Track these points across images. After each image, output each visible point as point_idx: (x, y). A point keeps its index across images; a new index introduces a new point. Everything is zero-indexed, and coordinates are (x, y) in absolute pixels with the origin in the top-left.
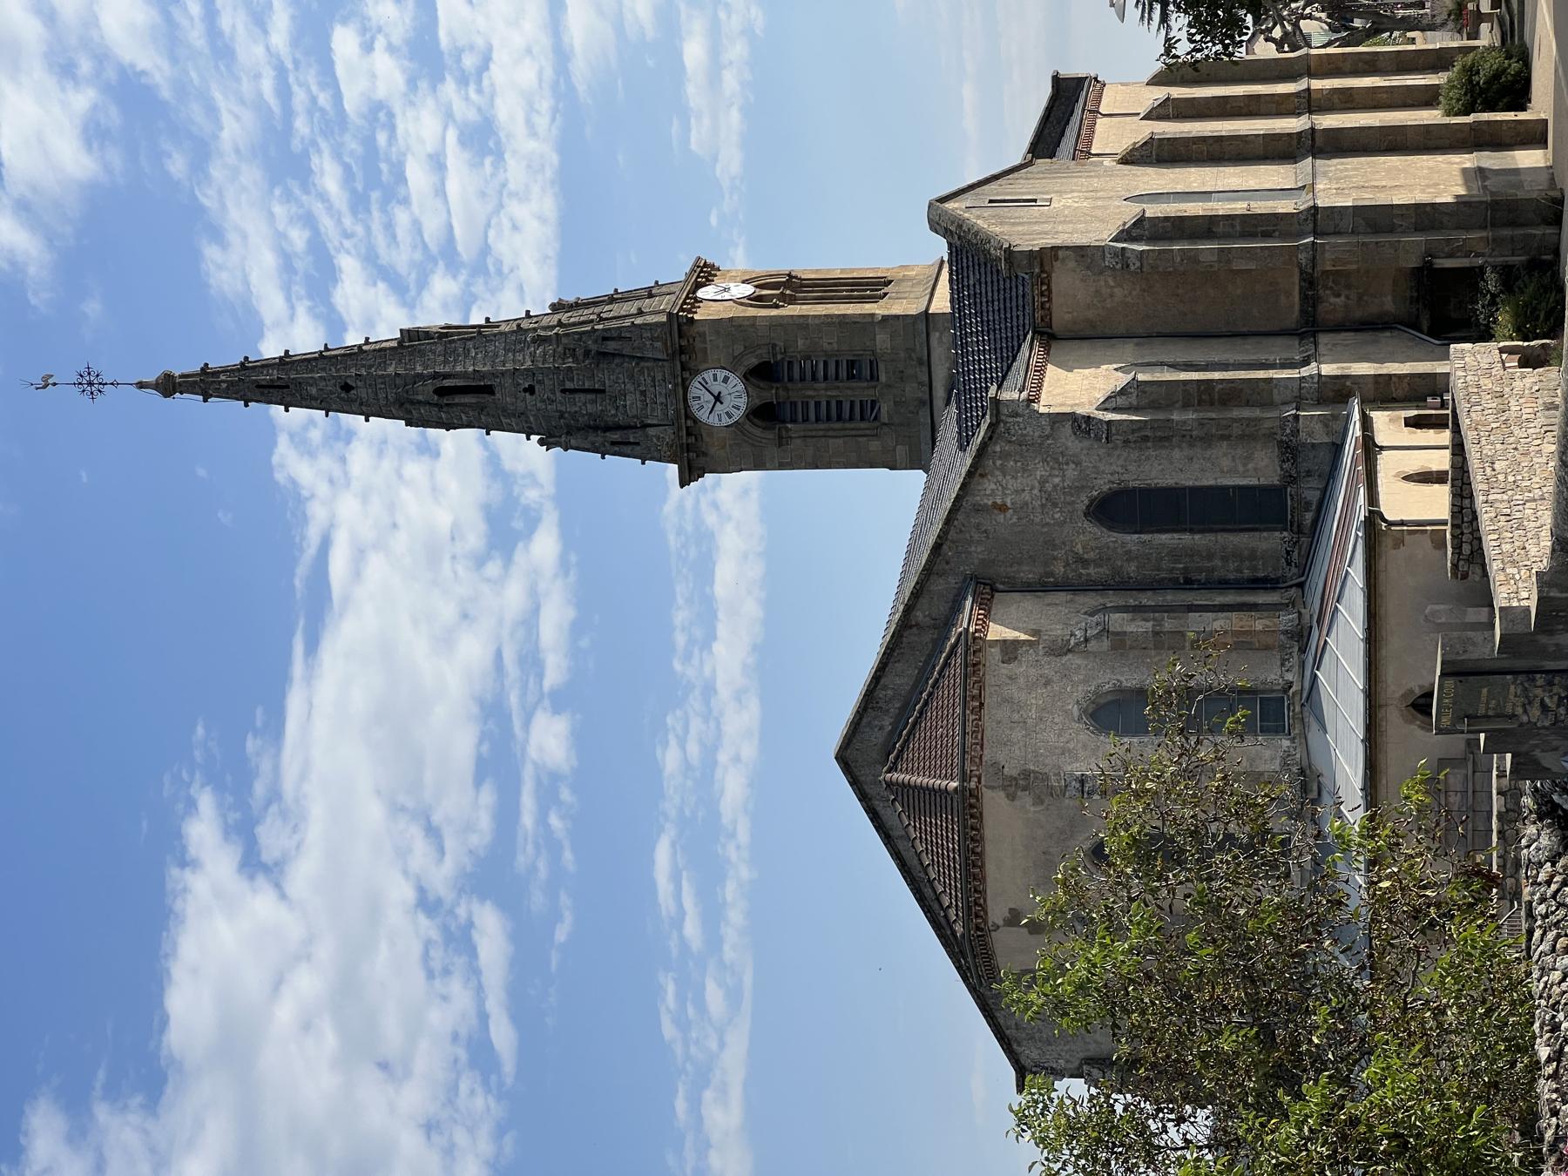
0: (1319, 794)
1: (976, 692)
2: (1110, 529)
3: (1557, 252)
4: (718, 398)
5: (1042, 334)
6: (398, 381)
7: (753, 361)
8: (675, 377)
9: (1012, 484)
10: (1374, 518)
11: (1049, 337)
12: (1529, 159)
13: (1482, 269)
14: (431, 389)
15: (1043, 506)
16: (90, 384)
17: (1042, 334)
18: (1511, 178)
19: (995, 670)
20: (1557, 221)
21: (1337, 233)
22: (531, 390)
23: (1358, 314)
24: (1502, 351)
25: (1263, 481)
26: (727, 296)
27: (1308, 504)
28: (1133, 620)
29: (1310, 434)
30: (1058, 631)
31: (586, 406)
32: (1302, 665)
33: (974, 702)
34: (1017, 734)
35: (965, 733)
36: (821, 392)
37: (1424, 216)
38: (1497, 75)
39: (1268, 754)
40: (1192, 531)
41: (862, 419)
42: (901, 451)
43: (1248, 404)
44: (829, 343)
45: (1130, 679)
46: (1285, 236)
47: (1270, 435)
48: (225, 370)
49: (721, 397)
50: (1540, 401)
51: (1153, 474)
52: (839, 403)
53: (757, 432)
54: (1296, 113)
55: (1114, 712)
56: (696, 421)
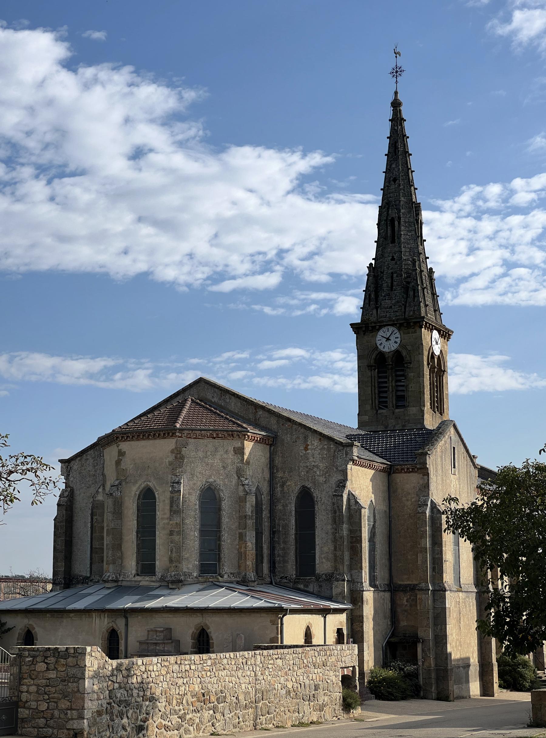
0: (171, 589)
1: (220, 435)
2: (297, 497)
3: (424, 698)
4: (388, 339)
5: (390, 469)
6: (398, 202)
7: (404, 354)
8: (397, 320)
9: (316, 452)
10: (284, 611)
11: (389, 472)
12: (475, 688)
13: (416, 664)
14: (394, 216)
15: (307, 467)
16: (397, 72)
18: (464, 680)
19: (230, 445)
20: (439, 699)
21: (434, 601)
22: (393, 259)
23: (399, 610)
24: (354, 667)
25: (317, 566)
26: (434, 343)
27: (307, 586)
28: (252, 506)
29: (336, 586)
30: (249, 472)
31: (386, 284)
32: (231, 582)
33: (215, 434)
34: (201, 454)
35: (201, 430)
36: (391, 384)
37: (441, 639)
38: (522, 676)
40: (296, 534)
41: (379, 402)
42: (366, 418)
43: (351, 559)
44: (412, 387)
45: (226, 505)
46: (433, 577)
47: (336, 569)
48: (403, 128)
49: (388, 341)
50: (320, 683)
52: (386, 392)
53: (374, 356)
55: (210, 498)
56: (378, 330)
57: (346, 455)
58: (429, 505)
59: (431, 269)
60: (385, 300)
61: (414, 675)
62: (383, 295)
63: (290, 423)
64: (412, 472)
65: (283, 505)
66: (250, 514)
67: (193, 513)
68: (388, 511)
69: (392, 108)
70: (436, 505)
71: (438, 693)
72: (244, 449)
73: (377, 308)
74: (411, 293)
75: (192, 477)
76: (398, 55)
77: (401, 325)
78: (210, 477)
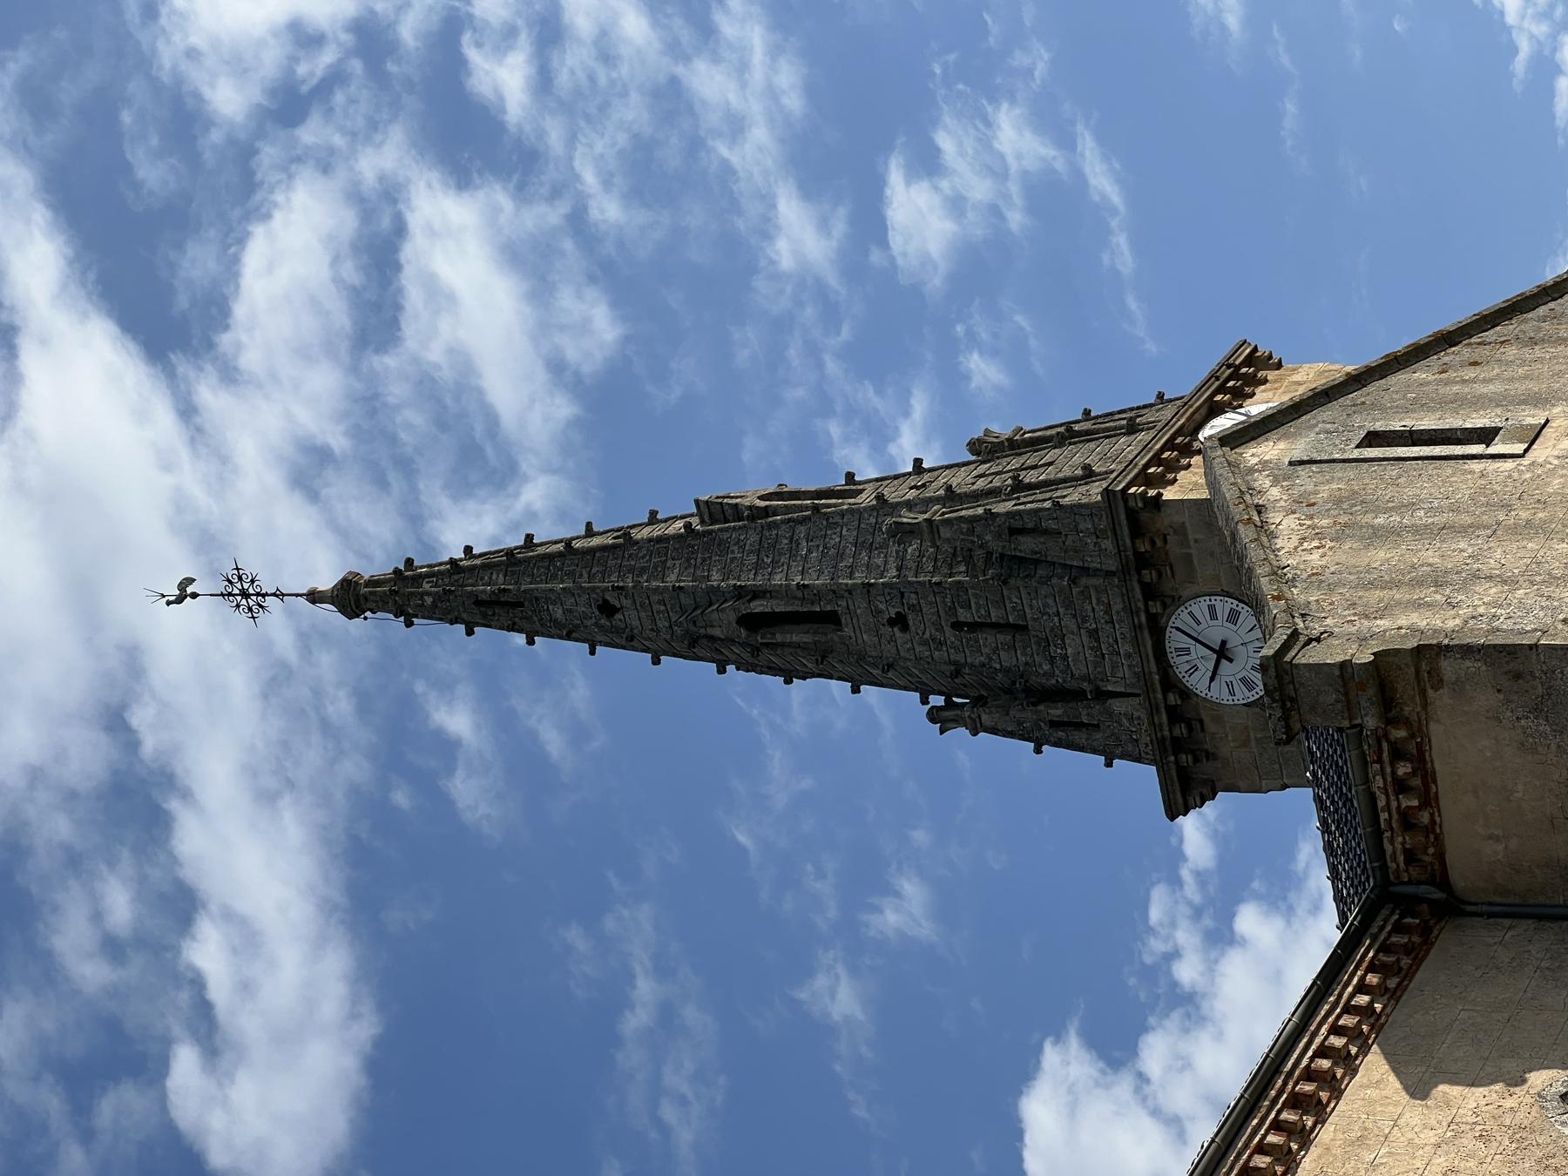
4: (1222, 653)
5: (1407, 904)
8: (1133, 613)
14: (733, 617)
16: (245, 594)
17: (1407, 904)
22: (900, 621)
56: (1186, 694)
59: (975, 446)
60: (1065, 657)
62: (1046, 667)
69: (368, 614)
73: (1102, 696)
74: (1027, 545)
76: (189, 590)
77: (1150, 592)
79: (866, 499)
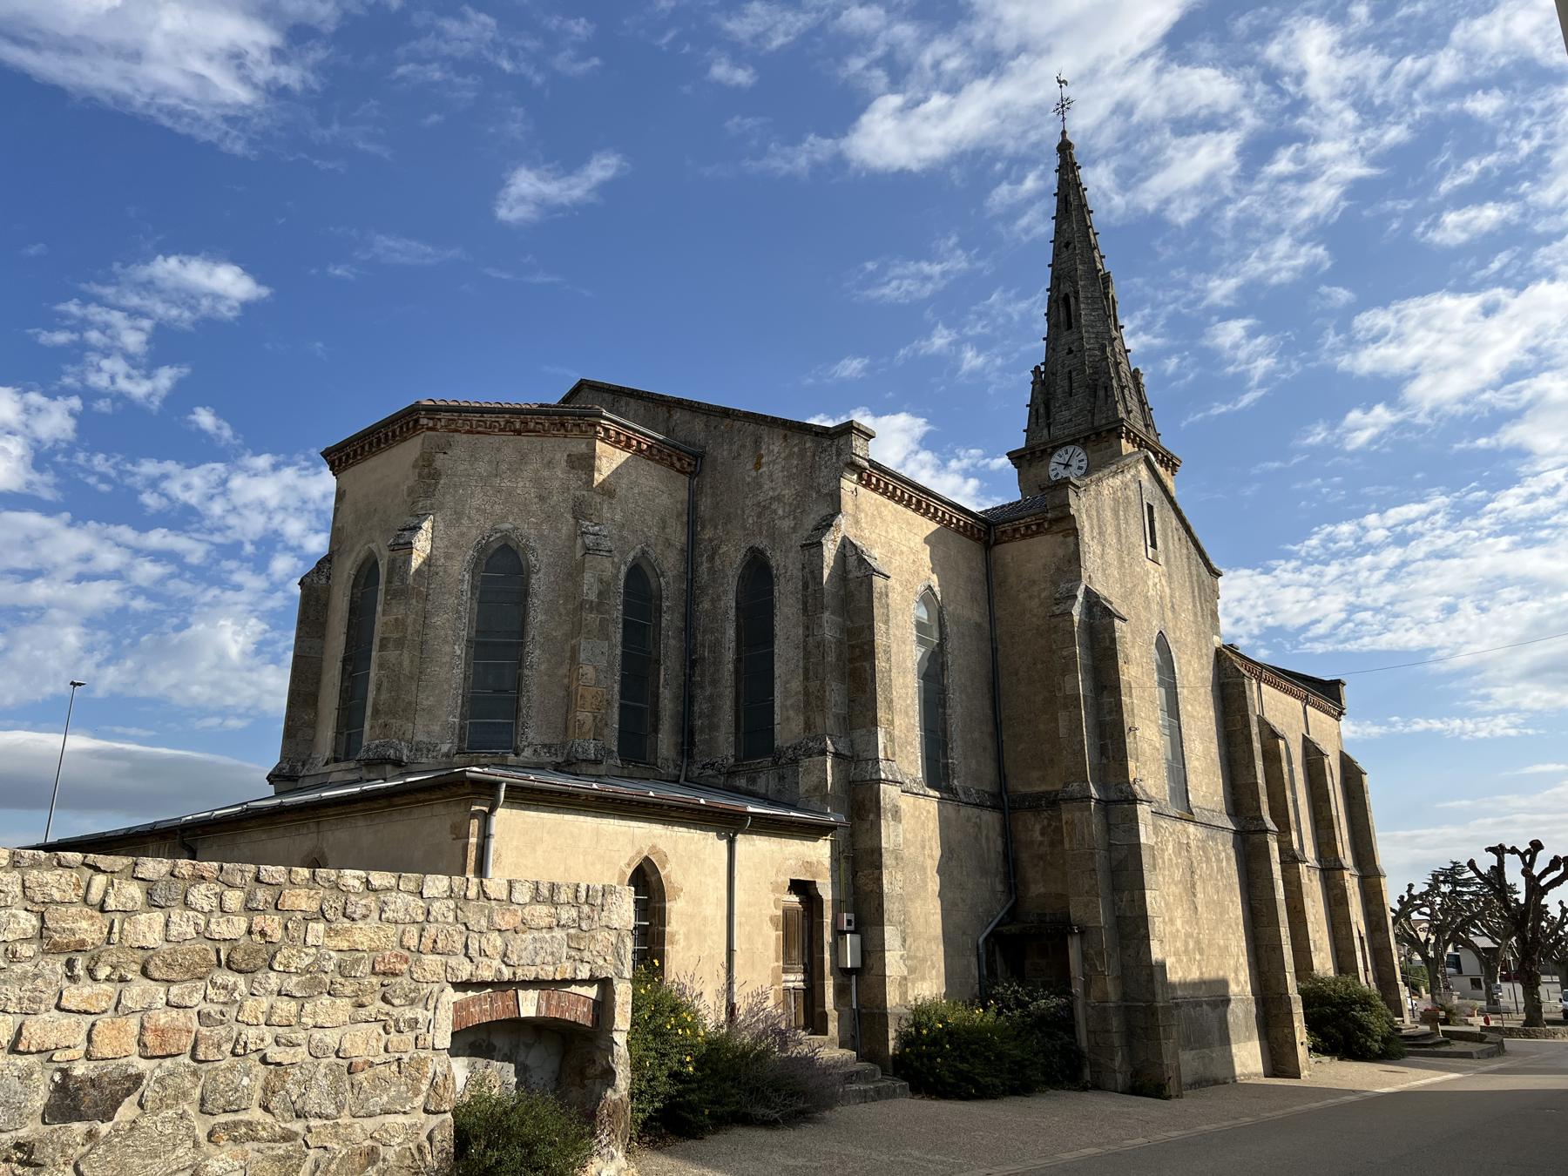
1: (532, 425)
3: (1097, 1086)
4: (1067, 466)
5: (988, 533)
12: (1248, 1057)
17: (988, 533)
18: (1217, 1036)
19: (559, 449)
21: (1109, 828)
22: (1070, 351)
23: (1025, 856)
25: (777, 728)
27: (753, 781)
29: (807, 771)
30: (613, 515)
34: (482, 468)
39: (437, 728)
40: (738, 661)
51: (786, 610)
54: (1320, 856)
56: (1051, 455)
57: (839, 455)
58: (1080, 598)
59: (1137, 370)
61: (1063, 1022)
63: (727, 421)
64: (1037, 533)
65: (712, 601)
66: (593, 597)
67: (452, 601)
68: (986, 625)
70: (1097, 597)
71: (1136, 1074)
72: (594, 457)
73: (1049, 426)
74: (1101, 393)
75: (458, 520)
77: (1087, 438)
78: (504, 518)
79: (1115, 334)
